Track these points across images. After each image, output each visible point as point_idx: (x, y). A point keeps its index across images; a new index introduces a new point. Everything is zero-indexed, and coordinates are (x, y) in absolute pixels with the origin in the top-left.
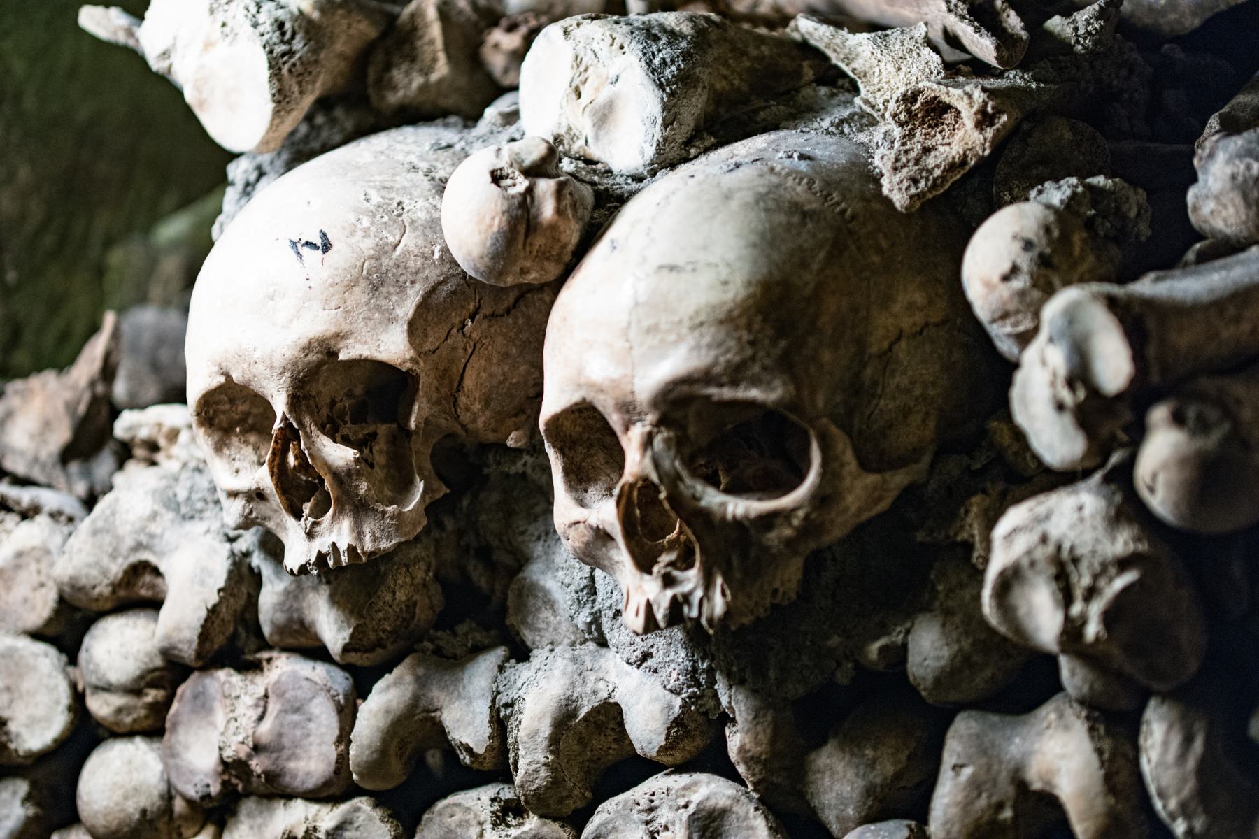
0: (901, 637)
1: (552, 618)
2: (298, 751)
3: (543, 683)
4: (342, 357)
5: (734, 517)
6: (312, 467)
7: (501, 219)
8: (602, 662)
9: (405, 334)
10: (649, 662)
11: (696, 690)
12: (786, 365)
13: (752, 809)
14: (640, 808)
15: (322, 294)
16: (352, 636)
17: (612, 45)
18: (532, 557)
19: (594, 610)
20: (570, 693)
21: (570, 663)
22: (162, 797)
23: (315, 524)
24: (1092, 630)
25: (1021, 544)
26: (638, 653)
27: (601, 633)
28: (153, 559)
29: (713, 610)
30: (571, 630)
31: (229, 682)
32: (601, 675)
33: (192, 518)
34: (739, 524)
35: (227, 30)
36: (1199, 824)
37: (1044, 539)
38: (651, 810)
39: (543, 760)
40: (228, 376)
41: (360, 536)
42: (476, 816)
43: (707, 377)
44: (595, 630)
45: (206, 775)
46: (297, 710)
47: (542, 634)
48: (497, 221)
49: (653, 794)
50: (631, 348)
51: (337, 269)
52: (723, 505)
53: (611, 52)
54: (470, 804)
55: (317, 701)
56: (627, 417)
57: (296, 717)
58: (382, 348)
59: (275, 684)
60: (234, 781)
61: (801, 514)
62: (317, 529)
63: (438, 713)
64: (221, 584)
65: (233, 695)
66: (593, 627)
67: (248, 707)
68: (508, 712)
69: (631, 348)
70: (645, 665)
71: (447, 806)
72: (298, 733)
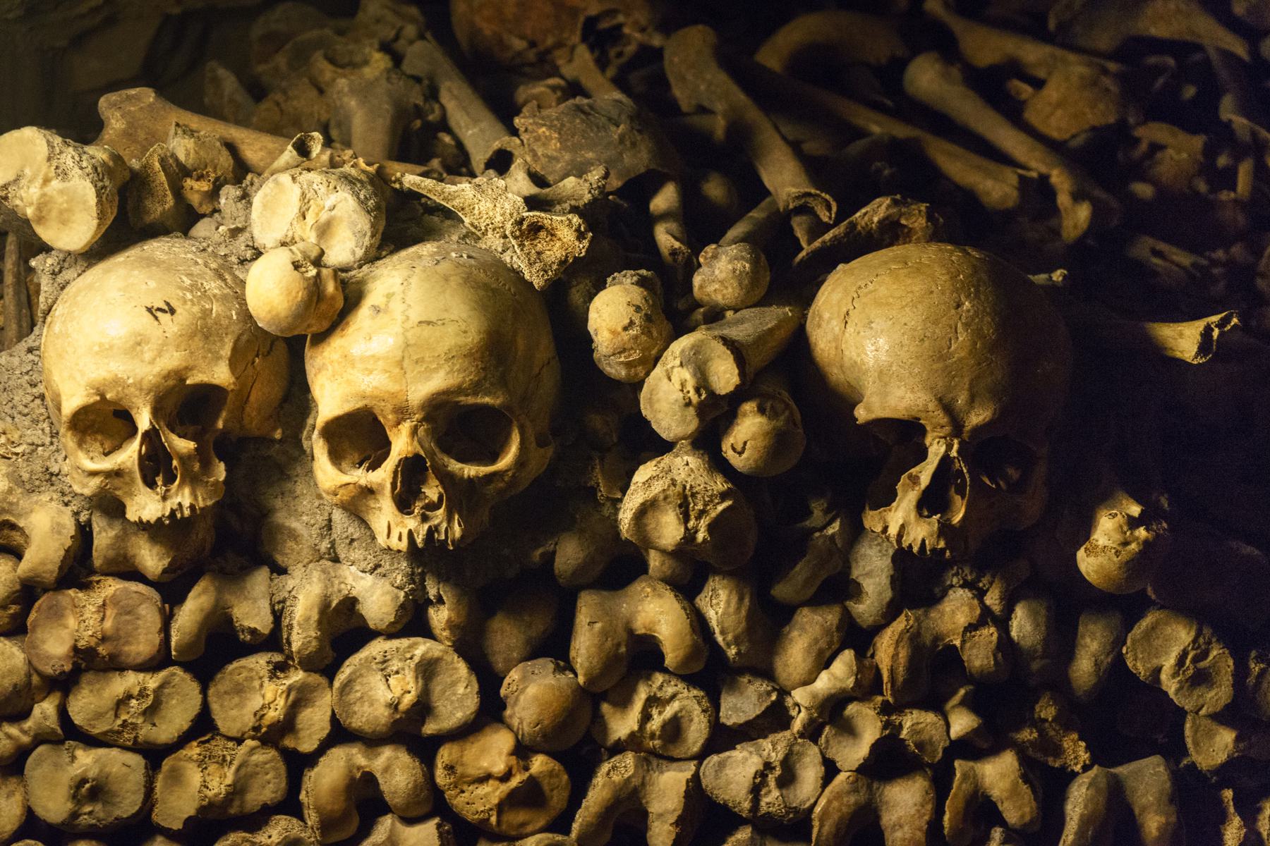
0: (552, 546)
2: (130, 639)
3: (308, 586)
4: (188, 382)
5: (469, 476)
6: (169, 453)
8: (340, 572)
9: (228, 367)
10: (379, 570)
12: (503, 382)
13: (456, 657)
14: (377, 661)
15: (175, 341)
16: (170, 564)
17: (328, 186)
18: (275, 509)
22: (25, 674)
23: (167, 491)
24: (701, 536)
25: (657, 487)
27: (335, 552)
28: (12, 519)
31: (78, 597)
32: (342, 580)
33: (33, 491)
34: (470, 480)
35: (59, 171)
36: (743, 649)
37: (674, 483)
38: (385, 662)
39: (314, 635)
40: (103, 396)
41: (196, 498)
42: (257, 673)
43: (459, 390)
45: (60, 659)
46: (129, 613)
48: (300, 294)
49: (386, 652)
51: (182, 325)
53: (328, 191)
54: (252, 666)
55: (143, 606)
56: (401, 416)
57: (128, 617)
58: (215, 376)
59: (112, 596)
60: (80, 661)
61: (510, 473)
62: (168, 494)
63: (230, 610)
64: (73, 533)
65: (81, 605)
66: (332, 550)
67: (93, 613)
68: (280, 606)
69: (405, 373)
70: (376, 572)
71: (236, 668)
72: (130, 627)
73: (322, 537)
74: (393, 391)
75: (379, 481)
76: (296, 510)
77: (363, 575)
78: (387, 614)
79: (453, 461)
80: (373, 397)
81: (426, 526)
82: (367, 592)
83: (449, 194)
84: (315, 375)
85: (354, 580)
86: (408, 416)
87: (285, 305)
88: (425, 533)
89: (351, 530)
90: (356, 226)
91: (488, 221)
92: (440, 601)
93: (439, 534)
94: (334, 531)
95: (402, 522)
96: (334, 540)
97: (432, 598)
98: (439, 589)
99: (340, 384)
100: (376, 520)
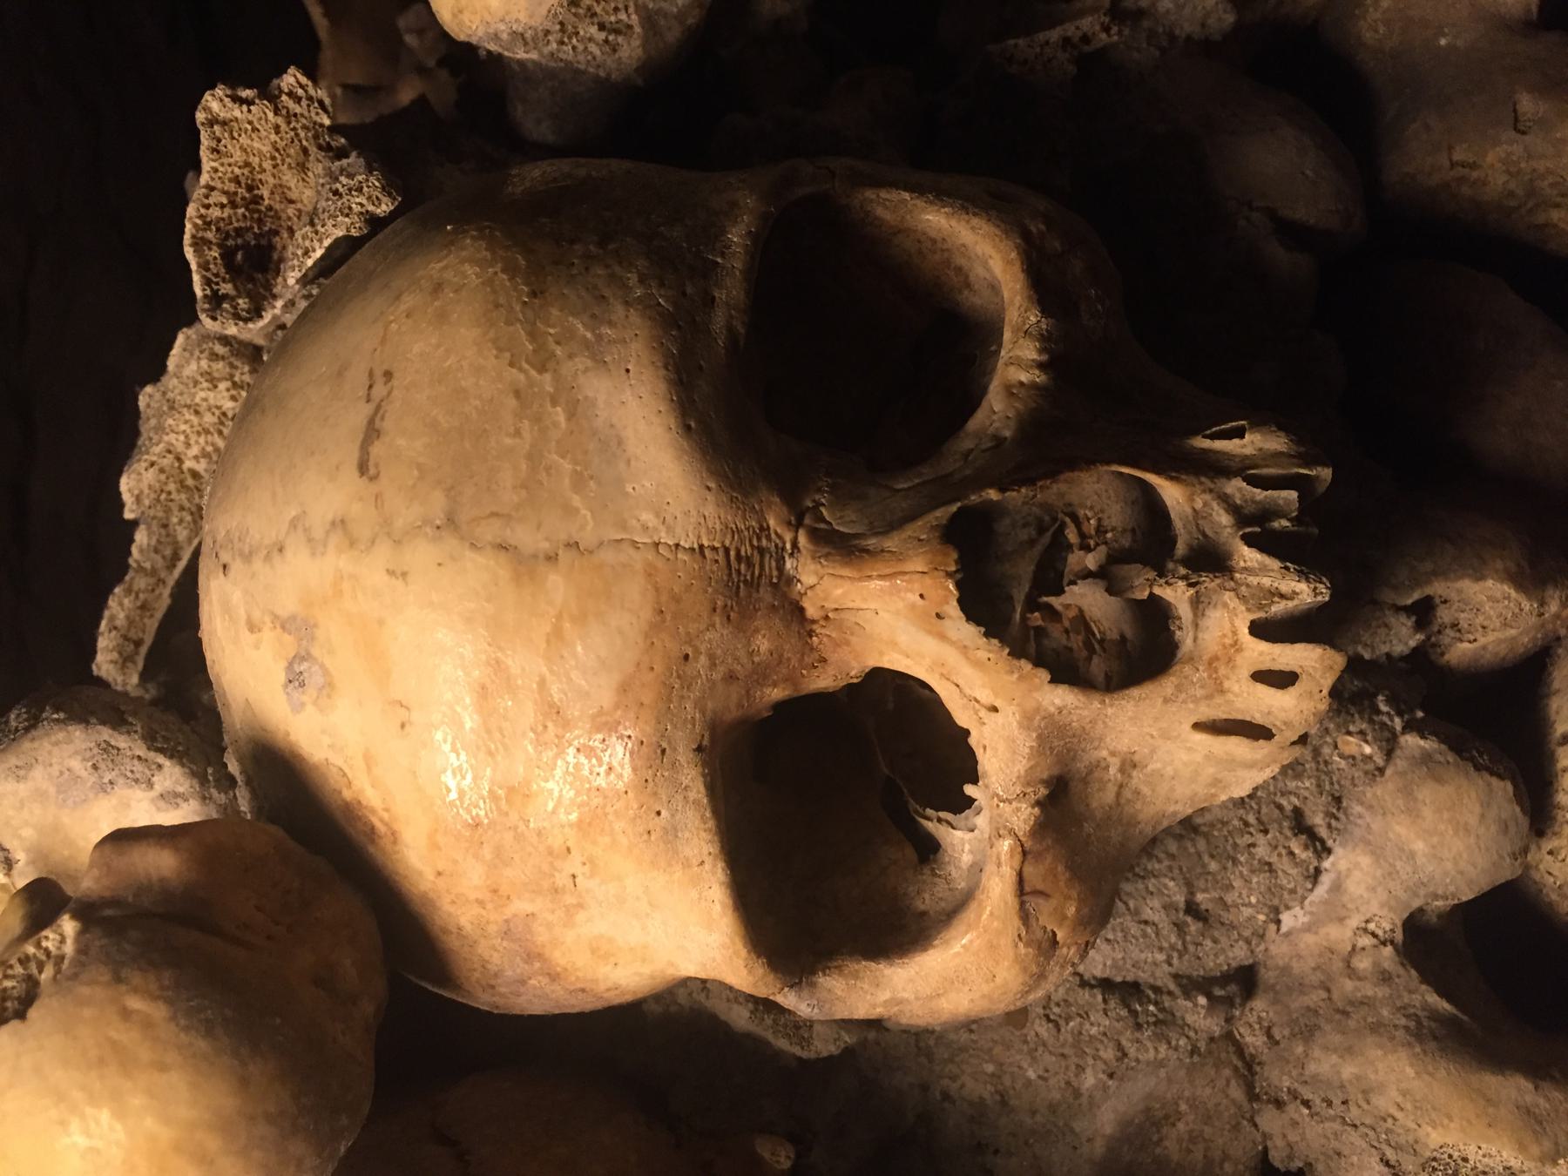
1: (1181, 1126)
3: (1383, 1103)
5: (1041, 366)
7: (135, 990)
10: (1318, 820)
11: (1380, 698)
19: (1177, 991)
20: (1400, 1034)
27: (1225, 979)
29: (1277, 455)
32: (1338, 965)
44: (1223, 987)
47: (1217, 1154)
48: (135, 1003)
50: (573, 545)
56: (765, 594)
66: (1218, 992)
69: (573, 545)
70: (1323, 832)
73: (1167, 1022)
74: (647, 614)
76: (1053, 1108)
77: (1326, 880)
78: (1486, 805)
79: (977, 421)
80: (667, 694)
81: (1248, 556)
82: (1392, 874)
83: (156, 551)
84: (554, 977)
87: (177, 1082)
88: (1275, 564)
92: (1423, 612)
93: (1277, 513)
94: (1143, 976)
96: (1176, 976)
97: (1412, 643)
98: (1399, 609)
99: (590, 861)
100: (1163, 789)
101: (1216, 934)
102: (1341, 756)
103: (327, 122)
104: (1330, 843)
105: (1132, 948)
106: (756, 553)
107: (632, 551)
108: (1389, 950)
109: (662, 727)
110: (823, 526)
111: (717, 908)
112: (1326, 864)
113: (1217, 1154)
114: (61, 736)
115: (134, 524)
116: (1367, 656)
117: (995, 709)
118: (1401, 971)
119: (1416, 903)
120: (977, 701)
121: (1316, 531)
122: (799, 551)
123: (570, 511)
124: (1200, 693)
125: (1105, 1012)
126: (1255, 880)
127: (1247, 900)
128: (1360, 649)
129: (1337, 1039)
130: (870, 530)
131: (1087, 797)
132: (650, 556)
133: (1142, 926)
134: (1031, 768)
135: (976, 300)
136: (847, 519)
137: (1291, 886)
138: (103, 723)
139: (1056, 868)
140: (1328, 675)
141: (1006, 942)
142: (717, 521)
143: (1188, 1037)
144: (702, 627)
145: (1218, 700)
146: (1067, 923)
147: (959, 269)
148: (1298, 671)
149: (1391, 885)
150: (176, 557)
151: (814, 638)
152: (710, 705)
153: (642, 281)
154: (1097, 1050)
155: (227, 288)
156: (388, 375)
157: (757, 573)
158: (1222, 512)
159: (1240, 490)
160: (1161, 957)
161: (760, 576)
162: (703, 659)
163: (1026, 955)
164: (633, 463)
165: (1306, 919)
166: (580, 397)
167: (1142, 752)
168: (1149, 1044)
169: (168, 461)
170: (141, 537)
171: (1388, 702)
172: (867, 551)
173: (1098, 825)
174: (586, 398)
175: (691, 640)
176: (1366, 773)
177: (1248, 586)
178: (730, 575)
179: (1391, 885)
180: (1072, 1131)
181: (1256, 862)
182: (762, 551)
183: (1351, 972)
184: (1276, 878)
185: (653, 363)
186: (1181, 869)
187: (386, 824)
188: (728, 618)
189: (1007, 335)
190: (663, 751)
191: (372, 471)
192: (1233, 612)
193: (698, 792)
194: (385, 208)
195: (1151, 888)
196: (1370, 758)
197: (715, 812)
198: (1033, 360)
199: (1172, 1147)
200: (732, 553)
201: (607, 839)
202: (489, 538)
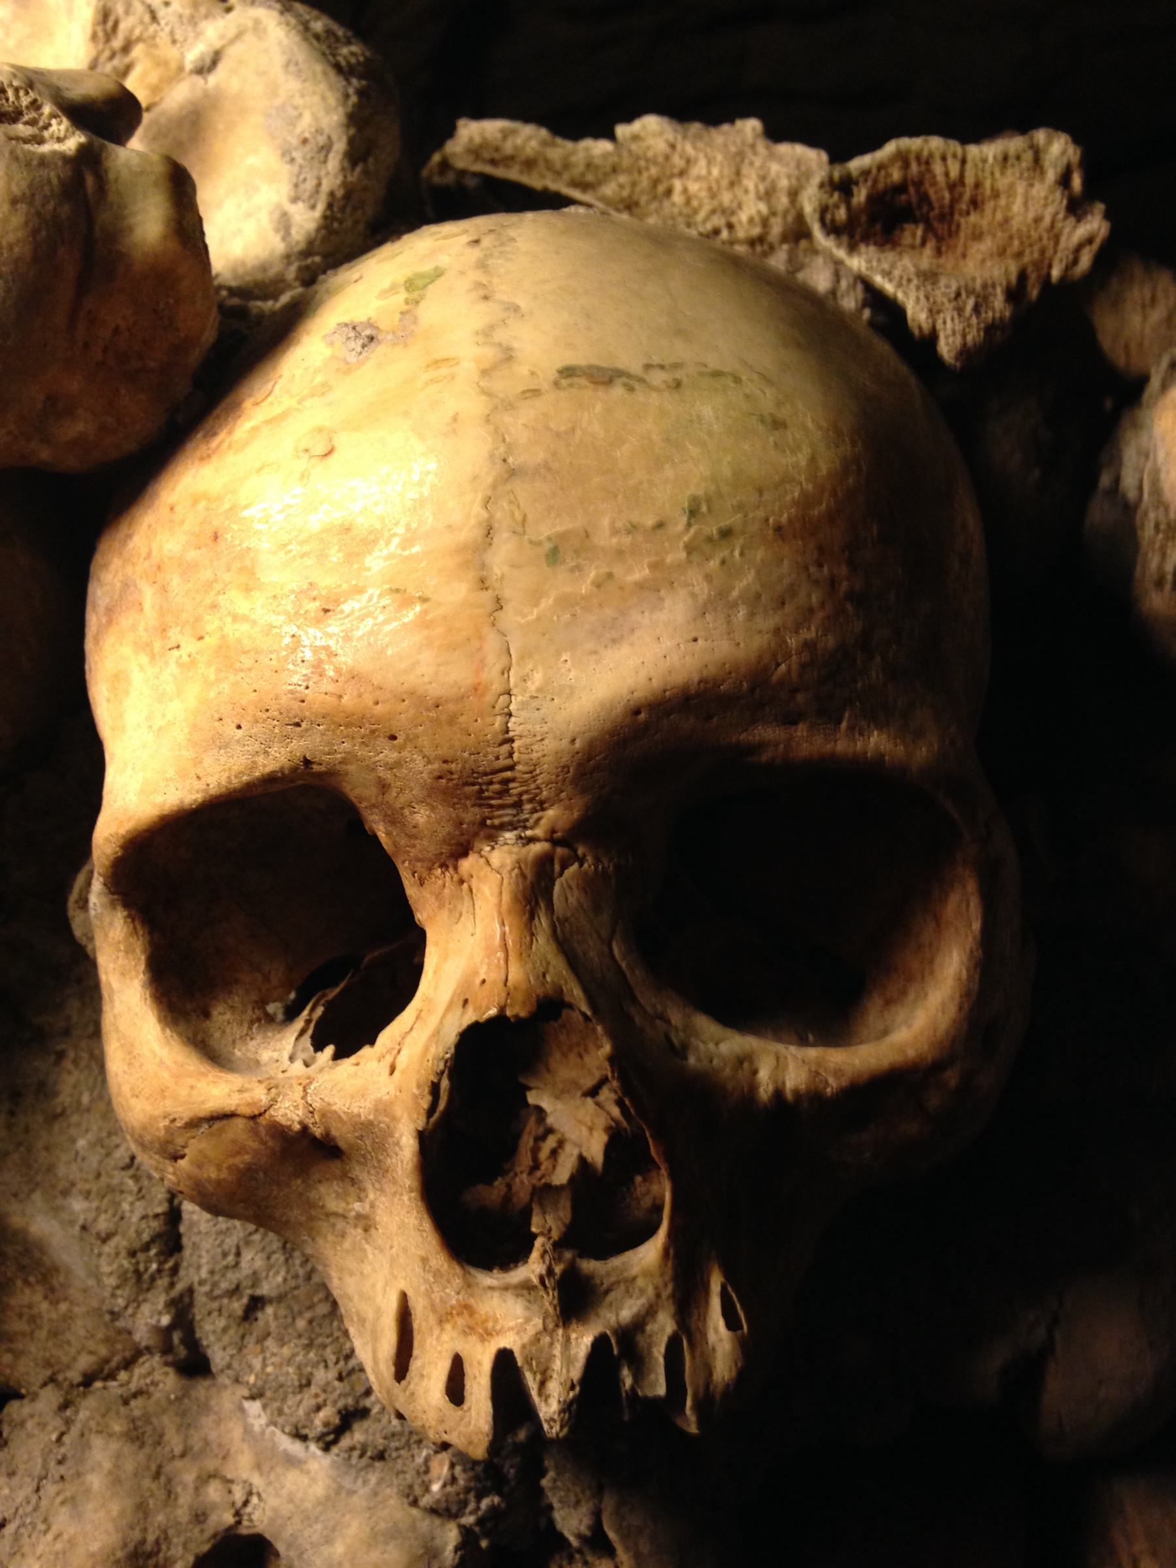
1: (45, 1306)
5: (778, 1094)
10: (357, 1435)
11: (496, 1499)
19: (175, 1293)
21: (128, 1449)
26: (328, 1414)
27: (193, 1343)
29: (709, 1370)
30: (100, 1335)
32: (211, 1464)
44: (182, 1341)
47: (19, 1346)
50: (499, 604)
52: (744, 1060)
56: (472, 814)
61: (952, 1077)
66: (176, 1337)
69: (499, 604)
70: (346, 1442)
73: (140, 1282)
75: (362, 1108)
76: (51, 1169)
79: (705, 1025)
81: (583, 1341)
82: (308, 1519)
83: (589, 165)
85: (258, 1466)
86: (507, 815)
88: (576, 1373)
89: (252, 1260)
90: (292, 122)
91: (718, 221)
93: (638, 1376)
95: (467, 1309)
96: (190, 1291)
98: (597, 1515)
100: (351, 1263)
101: (232, 1332)
102: (427, 1460)
103: (1056, 273)
104: (335, 1450)
105: (211, 1241)
106: (515, 799)
107: (498, 667)
108: (229, 1519)
109: (321, 721)
110: (557, 867)
111: (159, 799)
112: (313, 1448)
113: (19, 1346)
114: (332, 101)
115: (611, 137)
116: (545, 1482)
117: (392, 1070)
118: (208, 1534)
119: (280, 1547)
120: (399, 1052)
121: (626, 1418)
122: (524, 845)
123: (535, 596)
124: (436, 1296)
125: (144, 1217)
126: (291, 1370)
127: (269, 1362)
128: (551, 1474)
129: (129, 1466)
130: (558, 918)
131: (327, 1179)
132: (497, 687)
133: (233, 1250)
134: (340, 1117)
135: (873, 1016)
136: (569, 896)
137: (286, 1410)
138: (351, 142)
139: (247, 1153)
140: (462, 1439)
141: (168, 1105)
142: (540, 754)
143: (126, 1307)
144: (427, 751)
145: (432, 1320)
146: (196, 1171)
147: (904, 992)
148: (465, 1406)
149: (296, 1519)
150: (585, 186)
151: (439, 871)
152: (351, 768)
153: (808, 645)
154: (106, 1211)
155: (861, 195)
156: (678, 385)
157: (493, 802)
158: (635, 1310)
159: (663, 1329)
160: (204, 1273)
161: (491, 806)
162: (393, 756)
163: (158, 1129)
164: (594, 657)
165: (257, 1429)
166: (662, 592)
167: (378, 1235)
168: (115, 1266)
169: (678, 162)
170: (602, 147)
171: (493, 1509)
172: (532, 916)
173: (301, 1195)
174: (662, 599)
175: (410, 740)
176: (411, 1487)
177: (551, 1344)
178: (486, 774)
179: (296, 1519)
180: (32, 1191)
181: (309, 1369)
182: (518, 805)
183: (206, 1478)
184: (294, 1393)
185: (706, 666)
186: (297, 1288)
187: (218, 446)
188: (440, 777)
189: (812, 1053)
190: (298, 725)
191: (564, 382)
192: (520, 1330)
193: (264, 766)
194: (946, 348)
195: (274, 1257)
196: (427, 1489)
197: (249, 786)
198: (784, 1083)
199: (29, 1296)
200: (508, 774)
201: (212, 677)
202: (498, 515)
